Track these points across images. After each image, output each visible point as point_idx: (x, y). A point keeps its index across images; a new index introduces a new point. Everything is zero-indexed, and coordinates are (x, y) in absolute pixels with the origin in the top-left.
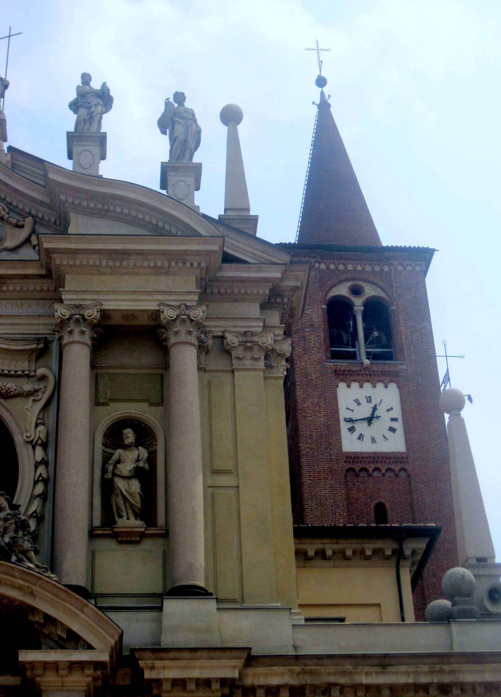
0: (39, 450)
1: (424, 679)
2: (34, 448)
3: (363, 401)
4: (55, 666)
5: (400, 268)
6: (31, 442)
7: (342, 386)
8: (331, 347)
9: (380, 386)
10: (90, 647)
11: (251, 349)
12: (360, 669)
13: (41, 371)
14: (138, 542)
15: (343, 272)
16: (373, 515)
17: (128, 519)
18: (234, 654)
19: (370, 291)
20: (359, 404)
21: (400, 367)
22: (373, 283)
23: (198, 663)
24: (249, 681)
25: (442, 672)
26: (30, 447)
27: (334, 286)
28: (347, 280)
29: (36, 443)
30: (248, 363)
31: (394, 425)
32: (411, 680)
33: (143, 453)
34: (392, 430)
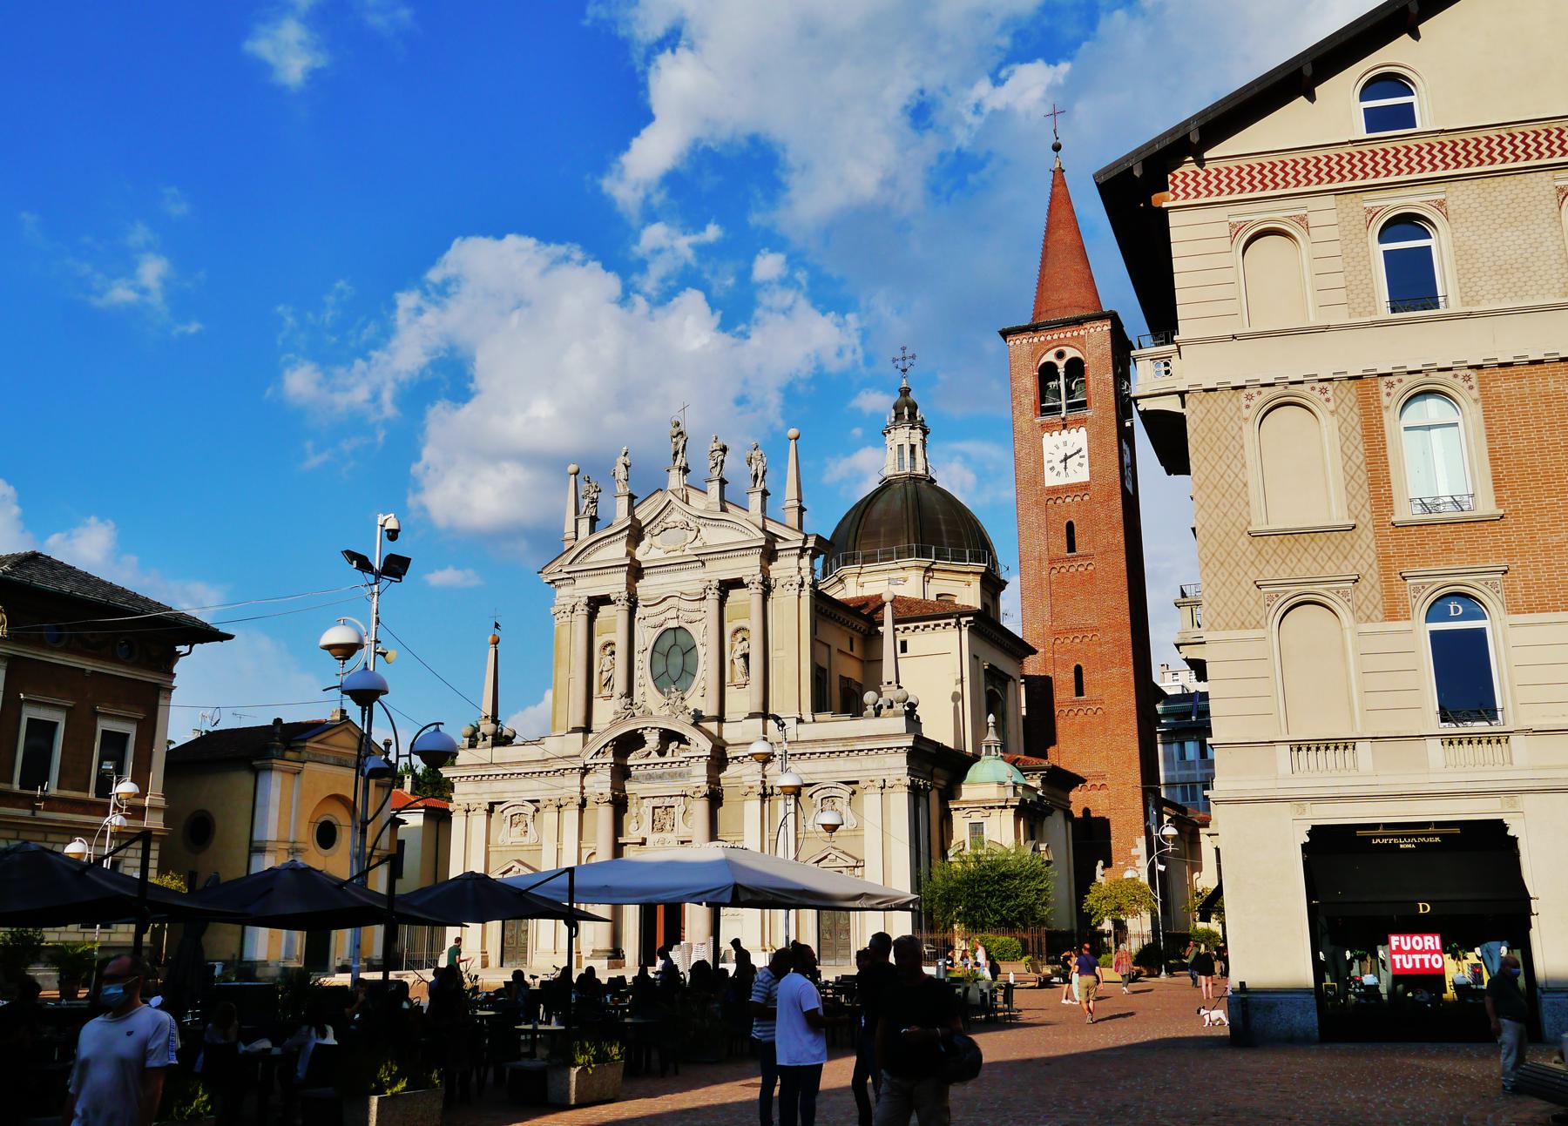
3: (1061, 445)
5: (1092, 330)
7: (1047, 435)
8: (1042, 403)
9: (1073, 431)
11: (791, 585)
13: (703, 609)
15: (1050, 342)
16: (1065, 531)
19: (1071, 353)
20: (1058, 448)
21: (1088, 414)
22: (1071, 346)
27: (1043, 355)
28: (1054, 347)
30: (791, 592)
31: (1082, 460)
34: (1080, 465)
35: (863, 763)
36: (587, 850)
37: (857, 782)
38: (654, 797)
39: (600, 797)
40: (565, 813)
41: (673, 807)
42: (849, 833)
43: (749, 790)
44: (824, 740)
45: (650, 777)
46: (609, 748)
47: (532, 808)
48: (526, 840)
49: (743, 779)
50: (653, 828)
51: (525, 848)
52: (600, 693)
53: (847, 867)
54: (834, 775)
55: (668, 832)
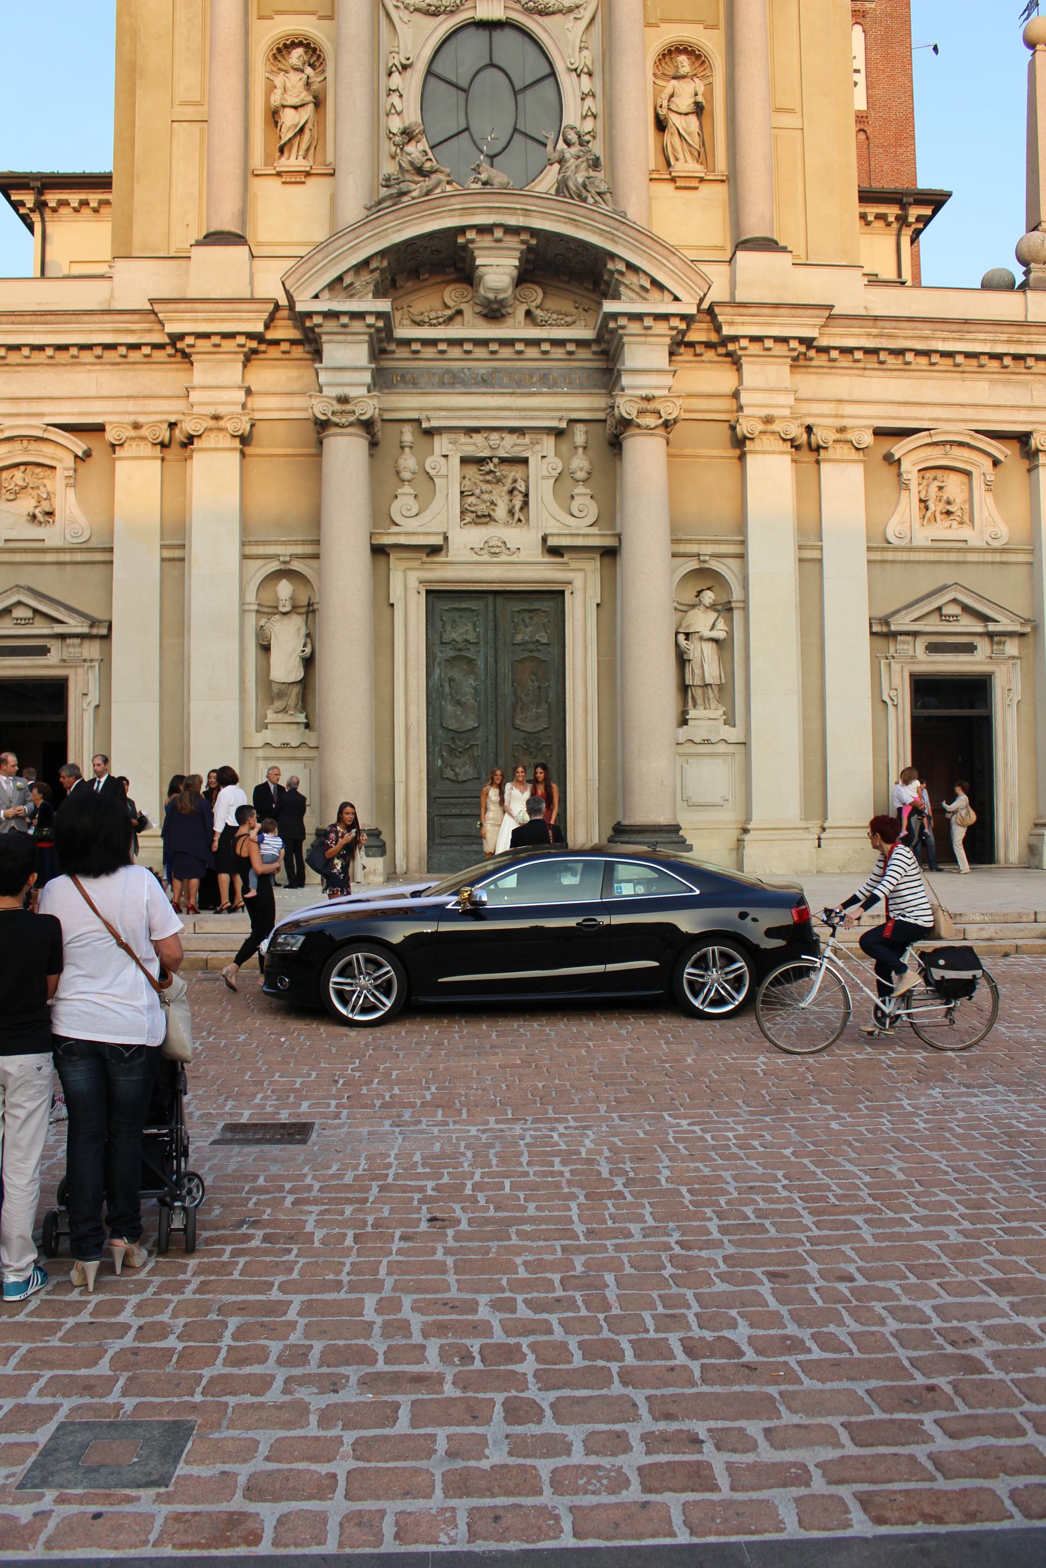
0: (585, 78)
1: (1000, 349)
2: (579, 76)
4: (638, 317)
6: (576, 70)
10: (676, 299)
12: (938, 334)
14: (696, 188)
17: (686, 162)
18: (816, 312)
23: (777, 320)
24: (824, 342)
25: (1019, 342)
26: (574, 74)
29: (582, 71)
32: (987, 350)
33: (699, 85)
35: (1034, 393)
36: (259, 563)
37: (1022, 439)
38: (470, 431)
39: (338, 407)
40: (195, 455)
41: (525, 461)
42: (989, 557)
43: (761, 427)
44: (966, 322)
45: (451, 381)
46: (366, 277)
47: (77, 444)
48: (52, 535)
49: (744, 398)
50: (463, 513)
51: (50, 557)
52: (268, 161)
53: (990, 635)
54: (969, 413)
55: (506, 524)
